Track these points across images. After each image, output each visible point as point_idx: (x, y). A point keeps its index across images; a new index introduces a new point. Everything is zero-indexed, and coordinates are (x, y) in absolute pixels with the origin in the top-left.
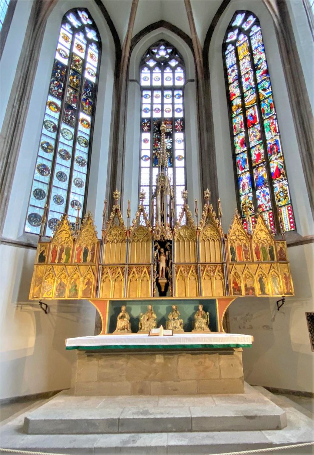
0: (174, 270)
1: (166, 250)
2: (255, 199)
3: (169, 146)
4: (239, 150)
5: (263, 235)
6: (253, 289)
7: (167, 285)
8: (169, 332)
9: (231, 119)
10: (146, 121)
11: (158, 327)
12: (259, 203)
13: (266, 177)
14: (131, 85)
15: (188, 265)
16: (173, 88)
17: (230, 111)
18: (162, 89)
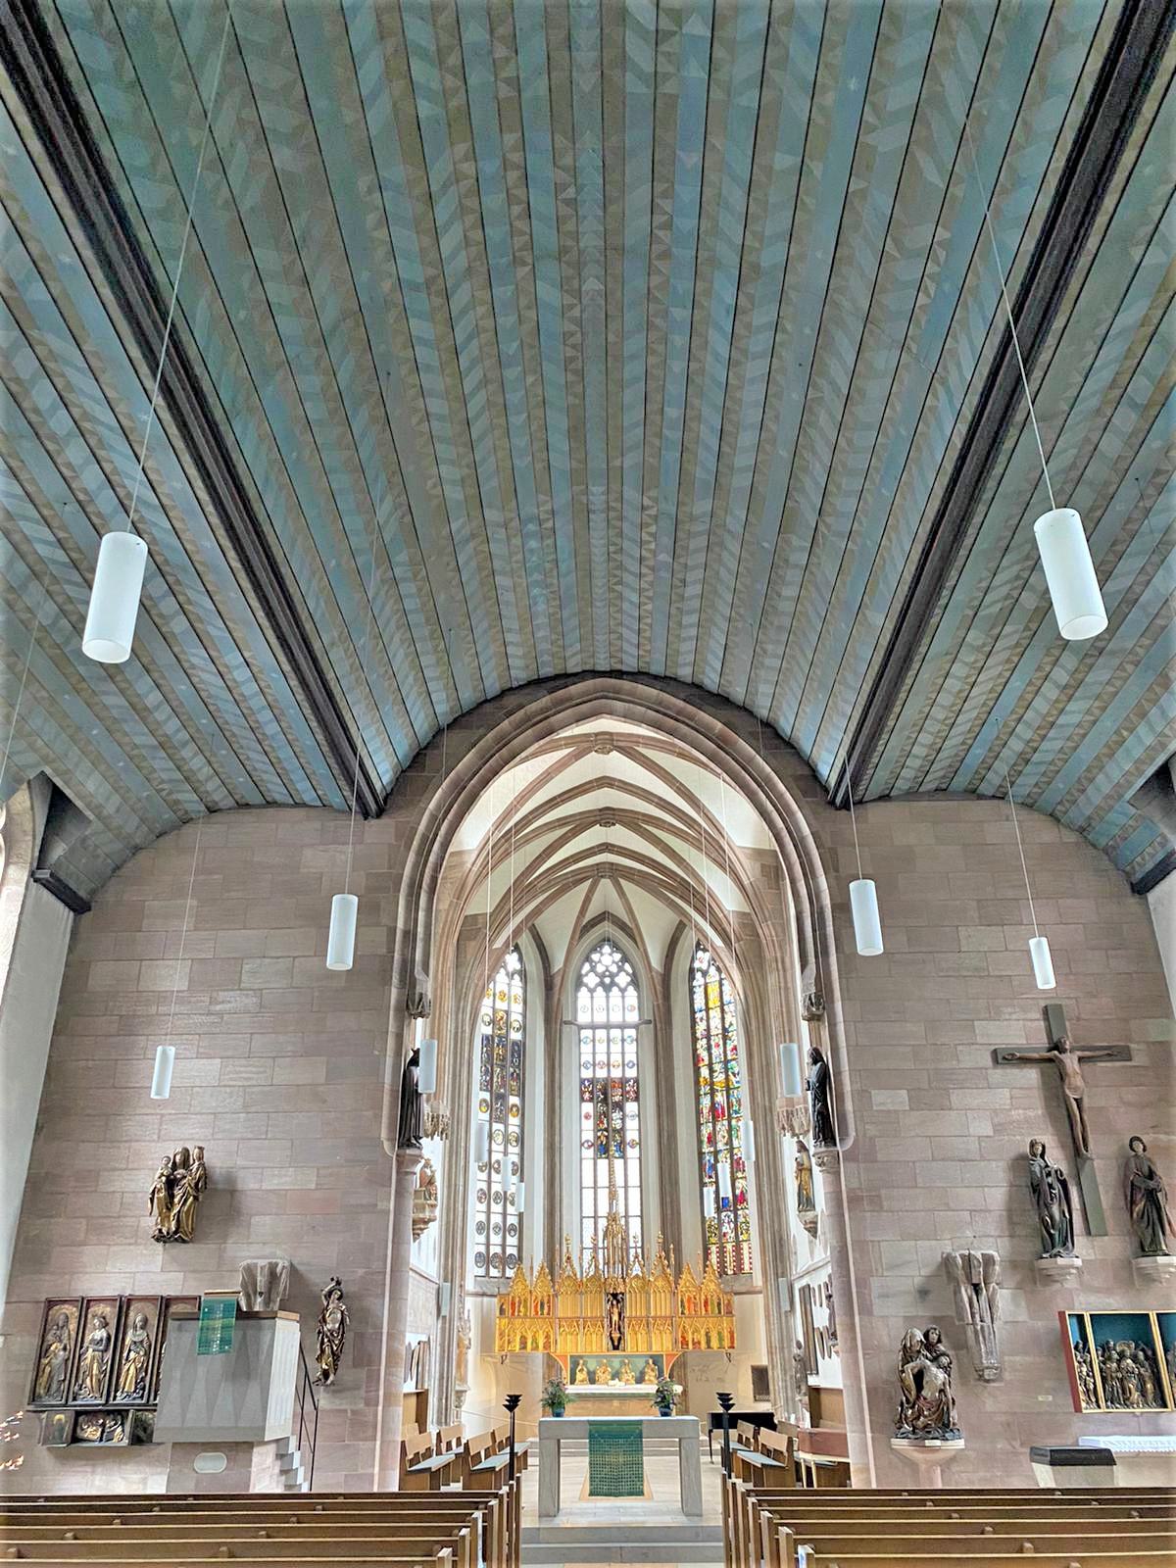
0: (626, 1325)
1: (618, 1302)
2: (720, 1223)
3: (617, 1124)
4: (706, 1149)
5: (712, 1286)
6: (699, 1343)
7: (620, 1339)
8: (623, 1383)
9: (698, 1097)
10: (587, 1083)
11: (613, 1379)
12: (724, 1230)
13: (731, 1198)
14: (566, 1029)
15: (639, 1319)
16: (622, 1027)
17: (697, 1083)
18: (608, 1027)
